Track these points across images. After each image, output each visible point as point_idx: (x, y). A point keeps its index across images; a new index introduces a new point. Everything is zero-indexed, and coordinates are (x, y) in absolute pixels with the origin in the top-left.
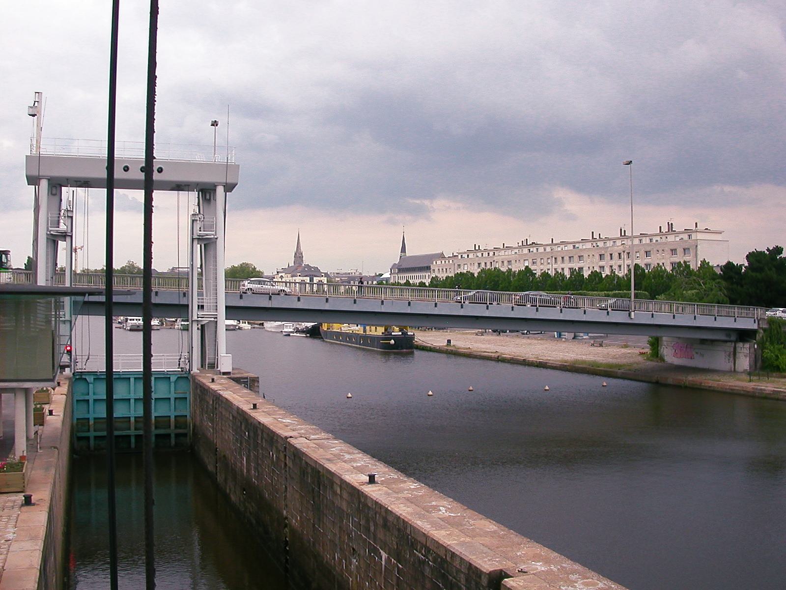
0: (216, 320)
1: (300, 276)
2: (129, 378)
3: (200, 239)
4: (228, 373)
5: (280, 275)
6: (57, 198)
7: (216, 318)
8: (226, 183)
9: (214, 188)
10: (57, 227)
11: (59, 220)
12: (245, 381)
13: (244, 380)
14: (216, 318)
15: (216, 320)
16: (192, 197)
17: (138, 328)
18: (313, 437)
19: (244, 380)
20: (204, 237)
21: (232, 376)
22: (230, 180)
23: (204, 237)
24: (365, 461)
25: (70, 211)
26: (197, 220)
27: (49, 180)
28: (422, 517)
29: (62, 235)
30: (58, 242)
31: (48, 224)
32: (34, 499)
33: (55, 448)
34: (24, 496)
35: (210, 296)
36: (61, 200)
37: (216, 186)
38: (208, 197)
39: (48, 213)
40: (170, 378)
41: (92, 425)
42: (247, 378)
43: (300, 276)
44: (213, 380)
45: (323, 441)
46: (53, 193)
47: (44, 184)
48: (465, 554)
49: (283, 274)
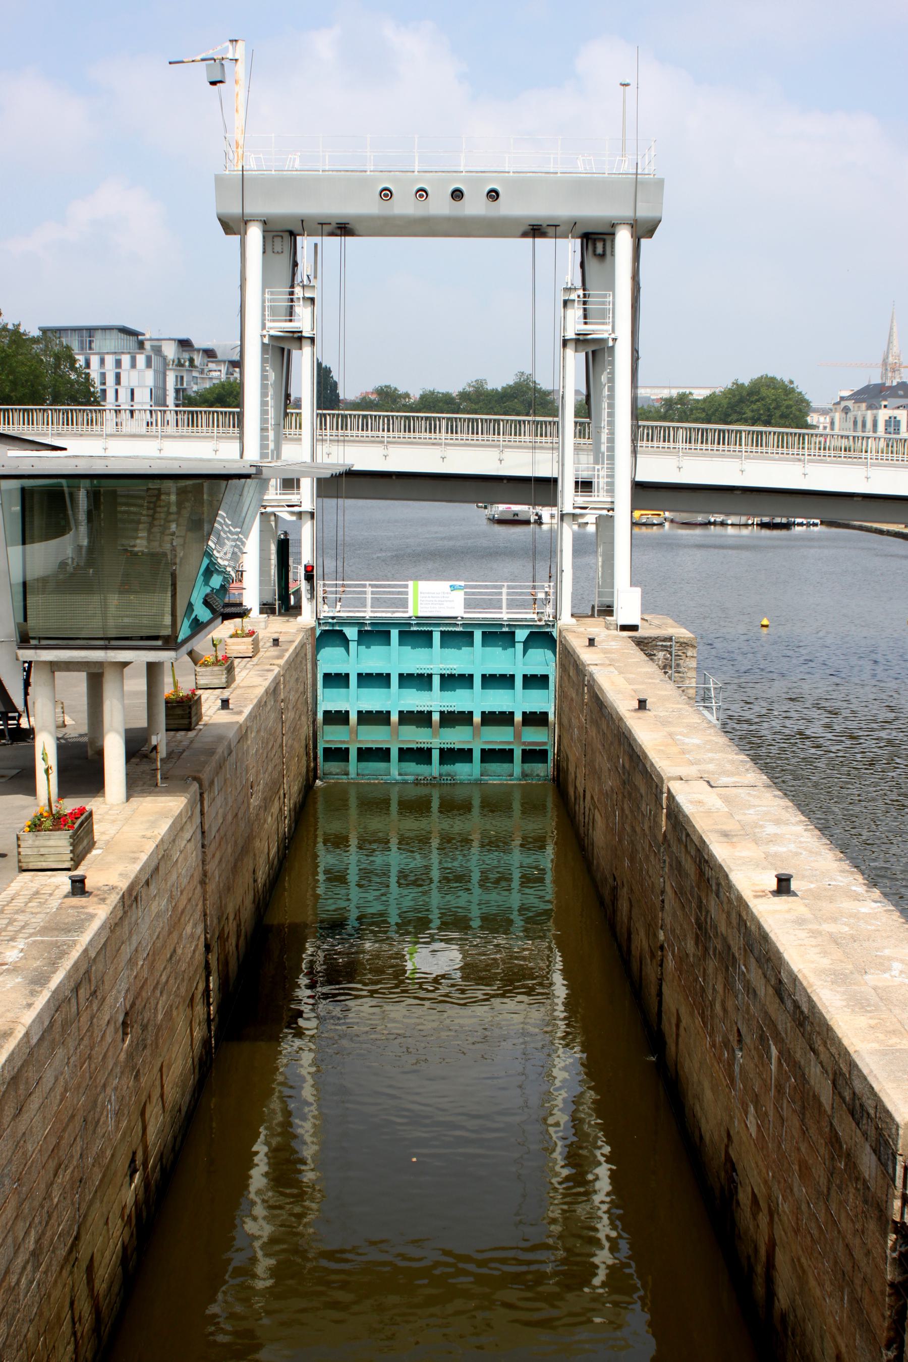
0: (610, 513)
1: (885, 406)
2: (430, 633)
3: (581, 341)
4: (634, 628)
5: (843, 404)
6: (284, 261)
7: (613, 509)
8: (636, 221)
9: (610, 230)
10: (286, 321)
11: (291, 307)
12: (665, 646)
13: (664, 644)
14: (613, 509)
15: (610, 513)
16: (571, 247)
17: (516, 518)
18: (725, 780)
19: (664, 644)
20: (589, 337)
21: (640, 633)
22: (644, 212)
23: (589, 337)
24: (801, 842)
25: (308, 286)
26: (574, 300)
27: (265, 222)
28: (838, 978)
29: (293, 338)
30: (289, 352)
31: (263, 315)
32: (89, 884)
33: (196, 779)
34: (70, 878)
35: (603, 464)
36: (295, 264)
37: (613, 226)
38: (600, 250)
39: (263, 293)
40: (514, 633)
41: (518, 722)
42: (670, 639)
43: (885, 406)
44: (591, 642)
45: (740, 790)
46: (276, 251)
47: (255, 234)
48: (878, 1076)
49: (850, 404)
